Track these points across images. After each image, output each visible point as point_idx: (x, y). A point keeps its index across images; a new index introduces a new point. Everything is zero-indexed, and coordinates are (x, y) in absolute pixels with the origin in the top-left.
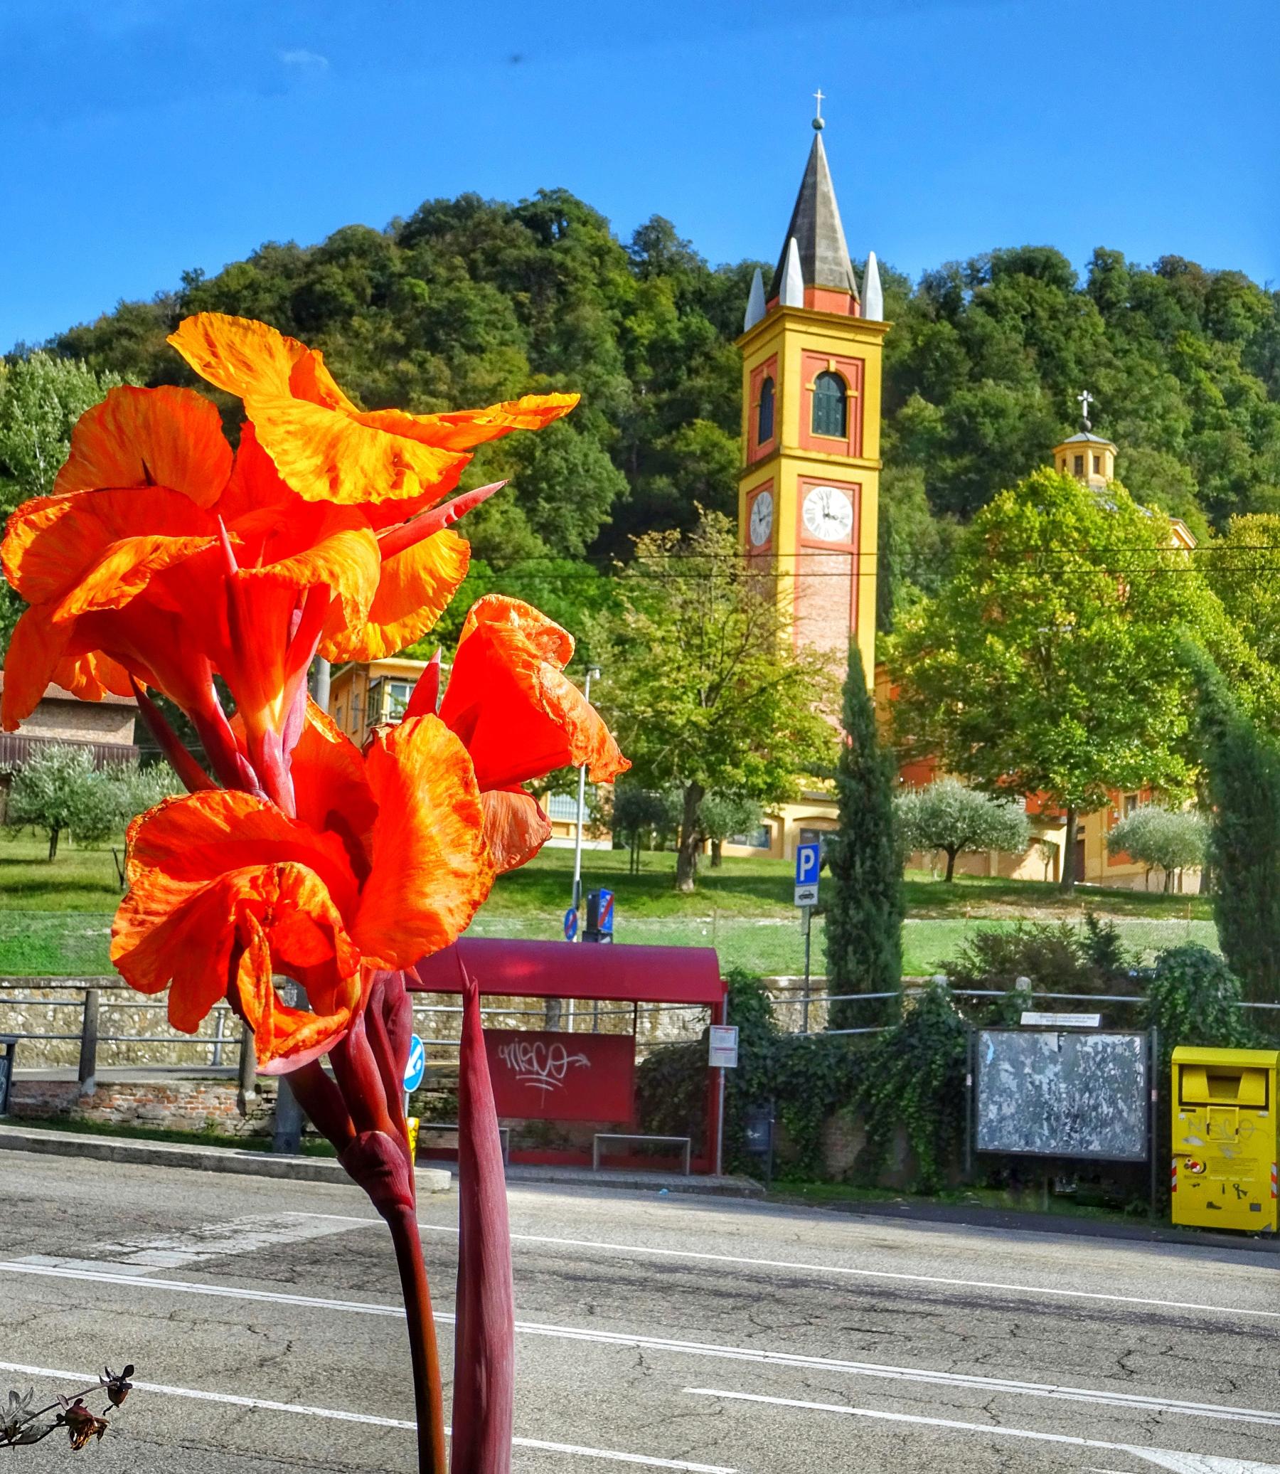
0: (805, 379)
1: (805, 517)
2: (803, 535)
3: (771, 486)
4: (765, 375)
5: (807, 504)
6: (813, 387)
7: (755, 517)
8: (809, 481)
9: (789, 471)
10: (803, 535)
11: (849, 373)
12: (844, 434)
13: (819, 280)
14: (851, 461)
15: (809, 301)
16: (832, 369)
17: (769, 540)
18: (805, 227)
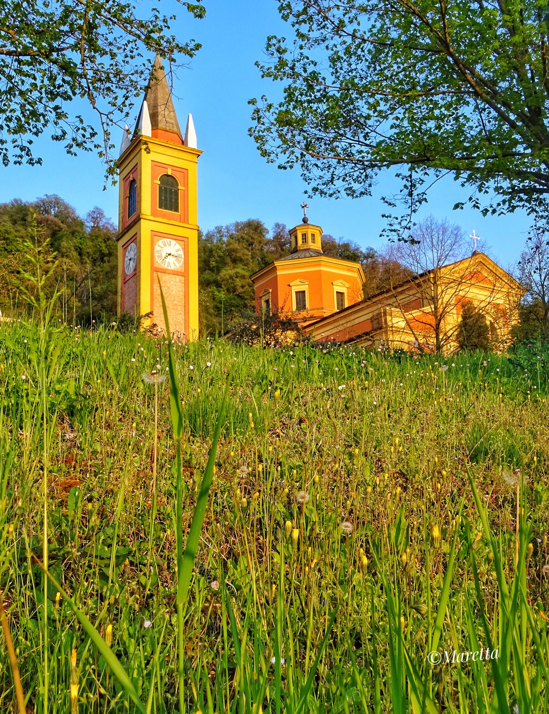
0: (153, 178)
1: (156, 255)
2: (155, 265)
3: (135, 239)
4: (131, 179)
5: (157, 248)
6: (159, 183)
7: (126, 259)
8: (156, 235)
9: (146, 227)
10: (155, 265)
11: (178, 176)
12: (176, 210)
13: (161, 125)
14: (181, 224)
15: (154, 135)
16: (169, 173)
17: (135, 270)
18: (152, 98)
